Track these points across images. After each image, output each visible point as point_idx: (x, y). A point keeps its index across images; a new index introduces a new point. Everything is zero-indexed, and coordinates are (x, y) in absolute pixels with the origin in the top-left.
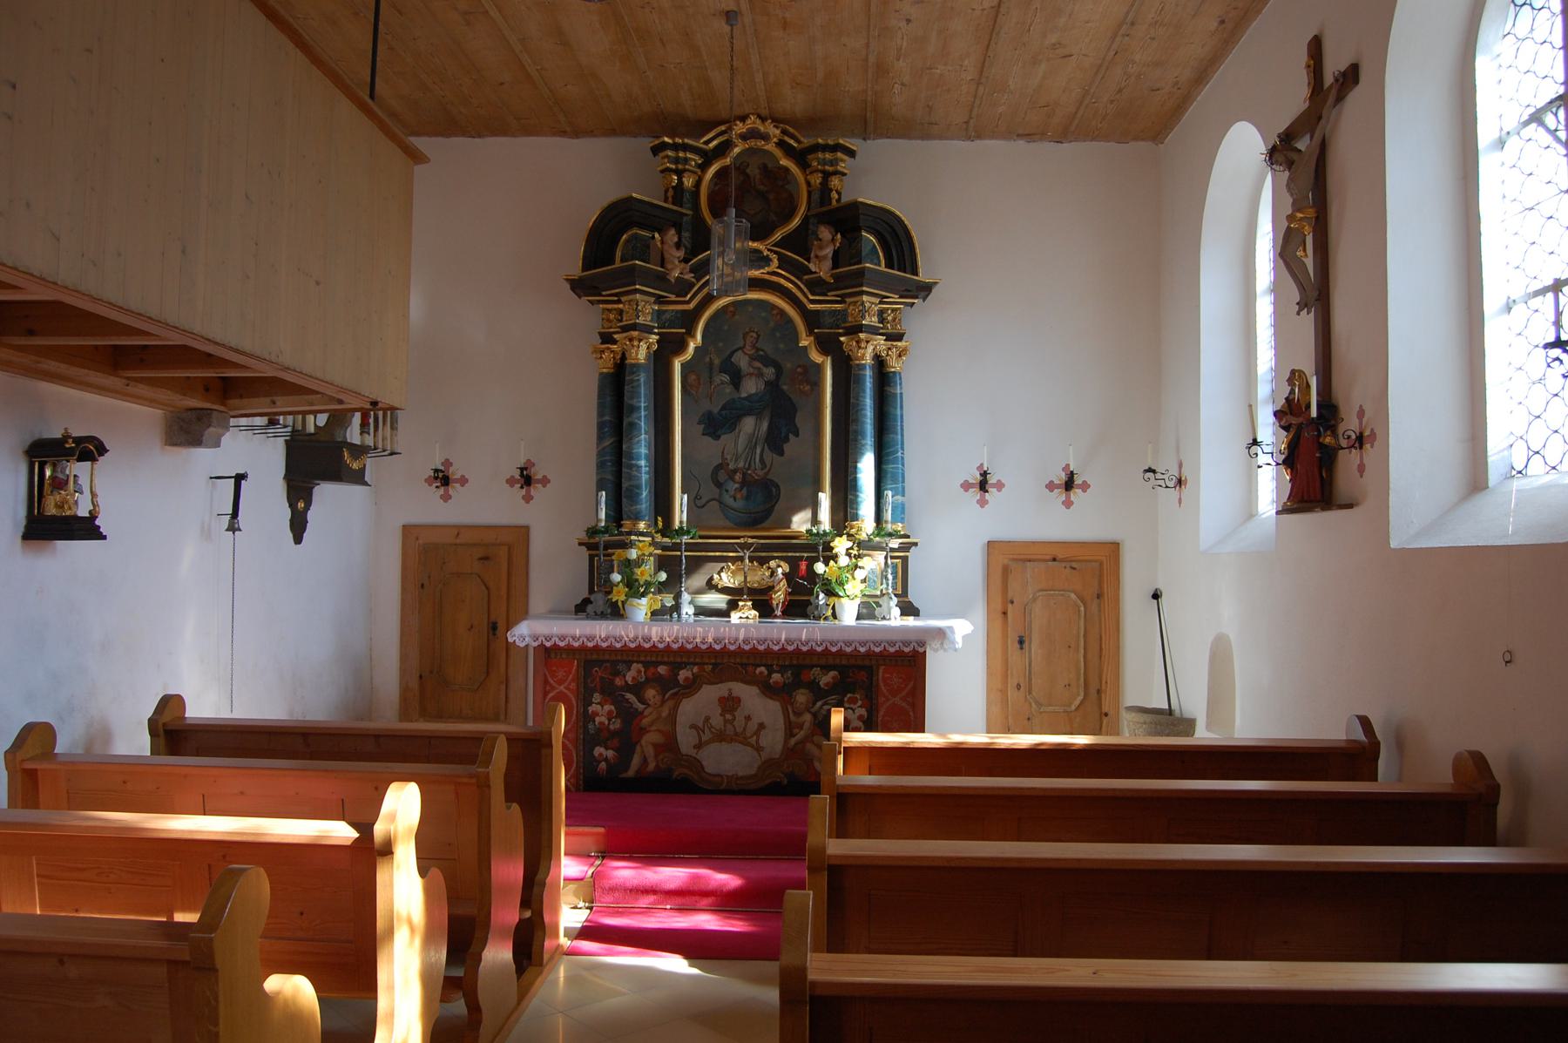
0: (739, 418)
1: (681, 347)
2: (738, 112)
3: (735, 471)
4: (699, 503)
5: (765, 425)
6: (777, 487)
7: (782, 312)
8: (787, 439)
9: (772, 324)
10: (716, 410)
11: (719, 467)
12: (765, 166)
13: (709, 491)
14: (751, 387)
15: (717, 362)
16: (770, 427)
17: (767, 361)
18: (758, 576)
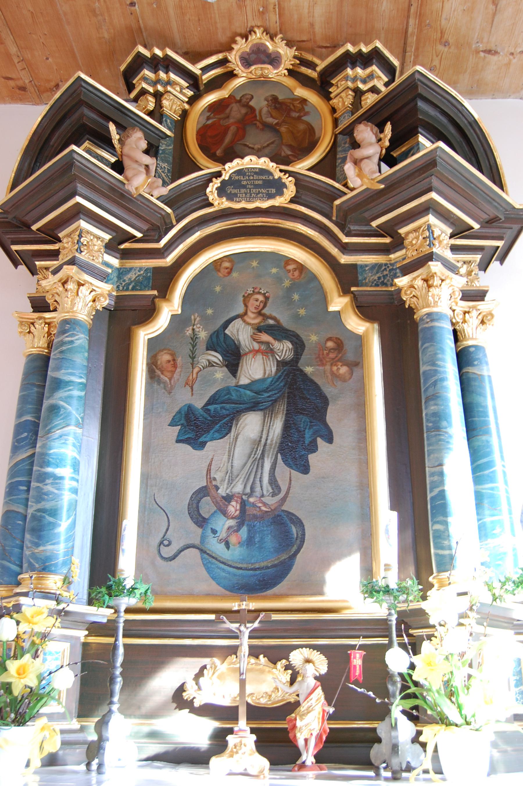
0: (234, 416)
1: (148, 313)
2: (239, 26)
3: (228, 499)
4: (167, 552)
5: (277, 426)
6: (299, 523)
7: (301, 268)
8: (313, 448)
9: (287, 283)
10: (199, 404)
11: (203, 492)
12: (275, 99)
13: (184, 531)
14: (256, 369)
15: (203, 335)
16: (286, 428)
17: (278, 332)
18: (267, 685)
